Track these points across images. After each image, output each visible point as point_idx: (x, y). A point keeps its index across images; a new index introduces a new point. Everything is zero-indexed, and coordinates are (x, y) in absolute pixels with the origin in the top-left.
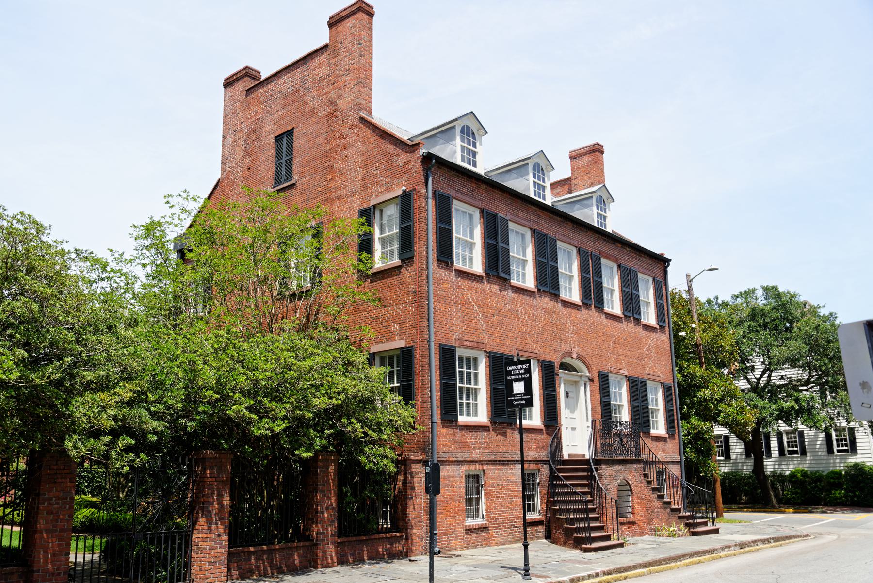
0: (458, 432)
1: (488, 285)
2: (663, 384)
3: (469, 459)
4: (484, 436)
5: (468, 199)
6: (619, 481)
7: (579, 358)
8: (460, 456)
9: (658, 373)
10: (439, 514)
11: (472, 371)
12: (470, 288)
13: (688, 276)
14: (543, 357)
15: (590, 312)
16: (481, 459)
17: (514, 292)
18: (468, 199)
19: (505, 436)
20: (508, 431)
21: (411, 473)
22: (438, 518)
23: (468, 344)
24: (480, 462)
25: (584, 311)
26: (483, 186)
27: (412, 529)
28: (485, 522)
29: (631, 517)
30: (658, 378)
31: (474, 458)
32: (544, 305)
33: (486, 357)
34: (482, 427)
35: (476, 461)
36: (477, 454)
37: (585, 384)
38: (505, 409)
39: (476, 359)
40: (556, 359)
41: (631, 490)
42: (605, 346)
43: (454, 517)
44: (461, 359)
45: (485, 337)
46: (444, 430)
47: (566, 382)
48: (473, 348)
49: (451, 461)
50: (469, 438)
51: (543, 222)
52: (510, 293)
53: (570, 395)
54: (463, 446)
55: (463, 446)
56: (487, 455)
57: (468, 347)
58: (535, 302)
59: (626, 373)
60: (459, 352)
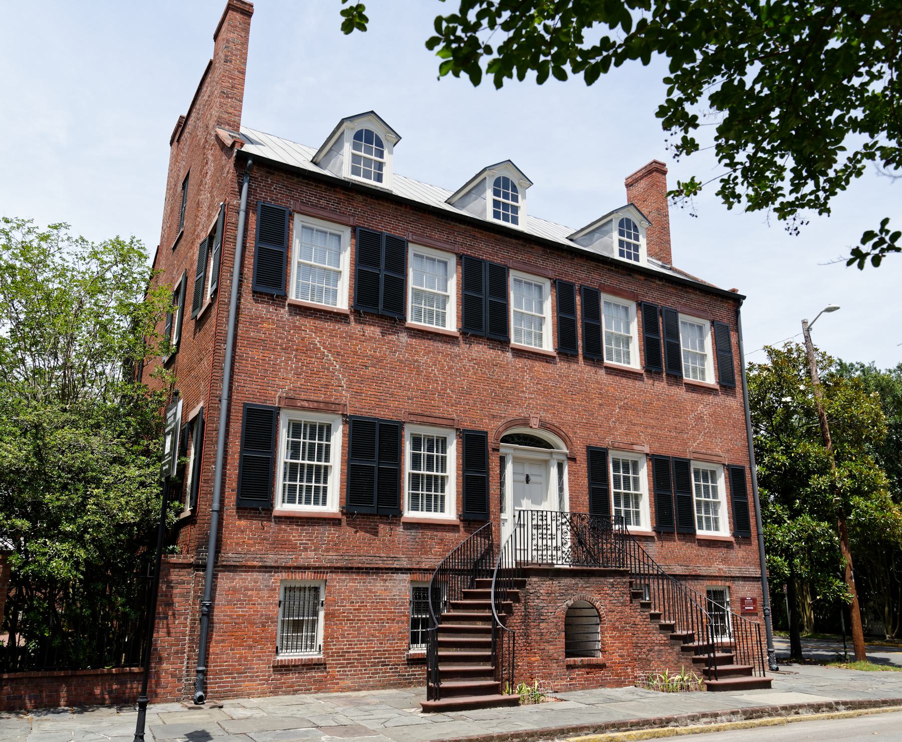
0: (272, 526)
1: (359, 327)
3: (290, 564)
4: (329, 533)
5: (326, 214)
6: (570, 603)
7: (544, 426)
8: (271, 559)
9: (717, 450)
10: (217, 642)
12: (317, 330)
13: (804, 322)
14: (467, 425)
15: (574, 366)
16: (317, 564)
17: (410, 336)
18: (326, 214)
19: (376, 534)
20: (382, 526)
21: (169, 583)
23: (306, 404)
24: (317, 569)
25: (562, 366)
26: (360, 198)
27: (160, 660)
28: (321, 656)
29: (599, 657)
30: (715, 458)
31: (301, 562)
32: (474, 355)
33: (345, 422)
34: (324, 519)
35: (308, 568)
36: (310, 557)
38: (374, 493)
39: (329, 427)
40: (493, 428)
41: (599, 616)
42: (604, 411)
43: (250, 647)
44: (697, 473)
45: (346, 396)
46: (243, 523)
47: (516, 461)
48: (316, 410)
49: (254, 567)
50: (295, 535)
51: (482, 246)
52: (404, 338)
53: (532, 478)
55: (280, 545)
56: (332, 558)
57: (303, 408)
58: (456, 350)
59: (647, 449)
60: (694, 465)
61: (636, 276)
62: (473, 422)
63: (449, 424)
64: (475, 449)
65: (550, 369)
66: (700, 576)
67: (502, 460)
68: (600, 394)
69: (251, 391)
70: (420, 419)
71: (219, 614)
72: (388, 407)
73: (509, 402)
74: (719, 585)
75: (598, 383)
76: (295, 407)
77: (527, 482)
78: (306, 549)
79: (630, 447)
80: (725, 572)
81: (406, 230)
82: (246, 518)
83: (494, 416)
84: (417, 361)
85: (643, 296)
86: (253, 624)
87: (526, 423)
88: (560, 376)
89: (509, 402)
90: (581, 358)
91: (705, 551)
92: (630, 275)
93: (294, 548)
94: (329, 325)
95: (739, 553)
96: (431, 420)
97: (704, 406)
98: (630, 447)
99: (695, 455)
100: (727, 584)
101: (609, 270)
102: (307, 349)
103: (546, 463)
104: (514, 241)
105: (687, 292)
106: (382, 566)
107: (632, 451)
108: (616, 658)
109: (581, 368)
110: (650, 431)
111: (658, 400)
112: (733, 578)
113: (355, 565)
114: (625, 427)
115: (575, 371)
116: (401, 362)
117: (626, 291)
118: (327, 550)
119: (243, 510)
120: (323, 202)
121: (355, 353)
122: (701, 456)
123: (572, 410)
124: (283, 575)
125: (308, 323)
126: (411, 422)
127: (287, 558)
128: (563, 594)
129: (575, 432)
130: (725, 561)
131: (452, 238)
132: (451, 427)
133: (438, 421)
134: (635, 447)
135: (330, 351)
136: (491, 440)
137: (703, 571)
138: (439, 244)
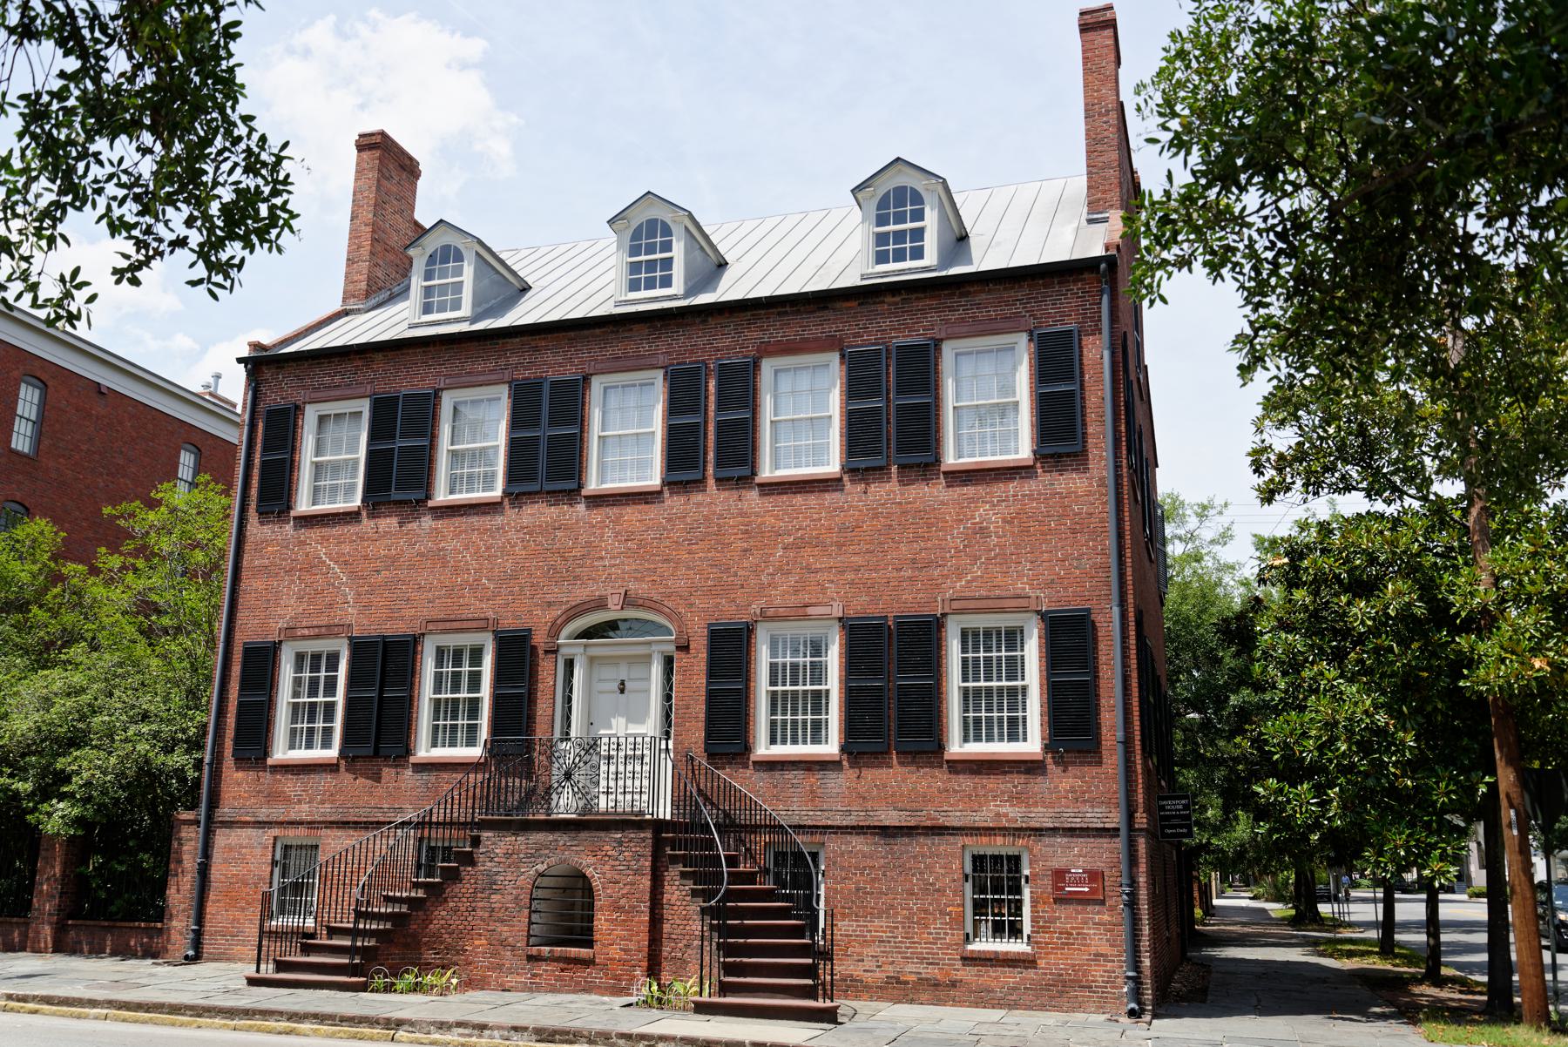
0: (267, 777)
1: (372, 523)
2: (1043, 616)
3: (281, 819)
4: (325, 781)
5: (338, 393)
6: (541, 868)
8: (263, 814)
9: (1022, 586)
11: (307, 675)
14: (508, 623)
15: (698, 497)
17: (436, 518)
19: (378, 780)
20: (386, 770)
21: (180, 839)
22: (210, 908)
23: (306, 632)
24: (311, 824)
26: (380, 356)
27: (171, 919)
31: (293, 816)
35: (301, 823)
36: (303, 811)
37: (668, 662)
38: (378, 731)
40: (538, 621)
43: (243, 909)
46: (240, 775)
48: (317, 637)
50: (291, 785)
51: (549, 357)
55: (274, 797)
56: (325, 811)
57: (304, 637)
58: (499, 520)
61: (838, 305)
62: (518, 617)
63: (482, 624)
64: (517, 656)
65: (652, 512)
66: (947, 828)
67: (570, 664)
69: (250, 630)
70: (441, 626)
71: (215, 873)
73: (577, 578)
74: (999, 846)
75: (742, 514)
76: (294, 638)
77: (622, 691)
78: (300, 802)
79: (801, 611)
81: (439, 374)
82: (243, 769)
83: (549, 604)
84: (443, 549)
85: (856, 335)
87: (601, 604)
88: (669, 520)
89: (577, 578)
90: (711, 482)
91: (966, 782)
92: (826, 308)
93: (288, 800)
94: (336, 531)
95: (1063, 781)
97: (990, 508)
98: (801, 611)
99: (956, 605)
101: (779, 314)
102: (312, 566)
103: (647, 660)
104: (598, 331)
105: (967, 294)
107: (806, 617)
108: (615, 952)
109: (713, 499)
110: (850, 576)
111: (876, 516)
112: (1039, 832)
113: (351, 819)
114: (792, 579)
115: (699, 505)
117: (816, 339)
118: (323, 802)
119: (241, 761)
120: (337, 379)
121: (366, 557)
122: (972, 604)
123: (689, 568)
124: (276, 832)
125: (314, 534)
126: (431, 632)
128: (532, 855)
130: (1016, 798)
131: (502, 362)
133: (465, 625)
134: (810, 610)
136: (540, 639)
137: (954, 820)
138: (481, 378)
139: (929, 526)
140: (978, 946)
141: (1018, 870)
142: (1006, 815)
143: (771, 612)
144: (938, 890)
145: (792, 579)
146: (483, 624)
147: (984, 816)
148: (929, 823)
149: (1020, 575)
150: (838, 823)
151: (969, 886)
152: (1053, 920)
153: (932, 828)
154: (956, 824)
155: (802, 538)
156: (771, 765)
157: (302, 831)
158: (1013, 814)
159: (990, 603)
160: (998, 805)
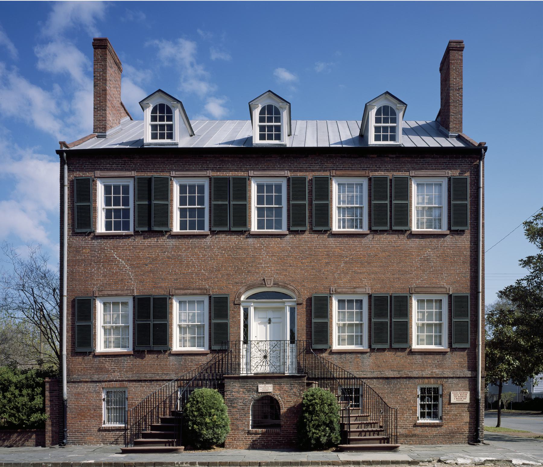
7: (276, 284)
8: (95, 378)
12: (116, 248)
14: (215, 292)
31: (112, 378)
36: (117, 375)
50: (108, 364)
54: (100, 370)
55: (100, 370)
62: (221, 289)
68: (328, 255)
72: (161, 287)
73: (249, 272)
74: (432, 384)
78: (114, 372)
80: (438, 374)
86: (89, 410)
88: (292, 248)
89: (249, 272)
93: (108, 371)
96: (189, 291)
98: (352, 290)
100: (439, 381)
102: (109, 261)
106: (158, 378)
107: (354, 293)
113: (142, 378)
114: (348, 277)
116: (169, 258)
118: (127, 372)
121: (139, 257)
122: (425, 290)
127: (105, 377)
129: (304, 286)
130: (439, 366)
132: (205, 294)
133: (195, 291)
134: (358, 290)
135: (123, 260)
137: (415, 374)
139: (406, 256)
140: (421, 421)
141: (438, 393)
142: (435, 372)
143: (339, 290)
144: (408, 401)
145: (348, 277)
146: (202, 291)
147: (427, 373)
148: (405, 376)
149: (443, 279)
150: (369, 376)
151: (419, 400)
152: (450, 411)
153: (406, 378)
154: (415, 376)
155: (352, 259)
156: (340, 353)
157: (117, 384)
158: (437, 372)
159: (431, 290)
160: (431, 369)
